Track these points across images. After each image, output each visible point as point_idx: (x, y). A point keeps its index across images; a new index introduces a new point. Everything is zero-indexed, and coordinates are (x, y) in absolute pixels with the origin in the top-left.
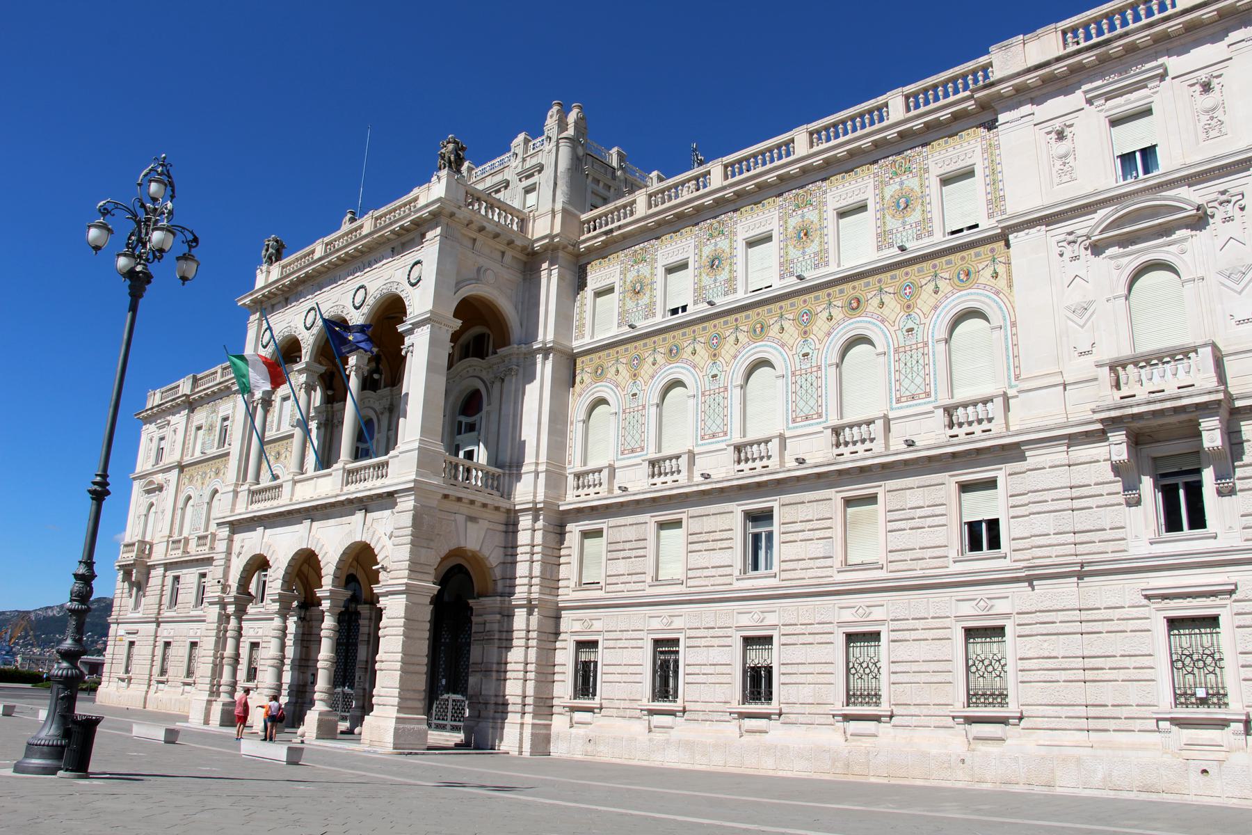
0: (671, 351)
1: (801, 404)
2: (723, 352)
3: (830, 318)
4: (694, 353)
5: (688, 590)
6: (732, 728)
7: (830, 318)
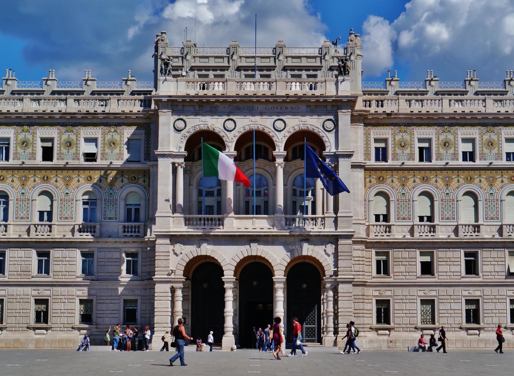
0: (424, 178)
1: (490, 213)
3: (502, 182)
4: (436, 181)
5: (440, 281)
6: (463, 333)
7: (502, 182)
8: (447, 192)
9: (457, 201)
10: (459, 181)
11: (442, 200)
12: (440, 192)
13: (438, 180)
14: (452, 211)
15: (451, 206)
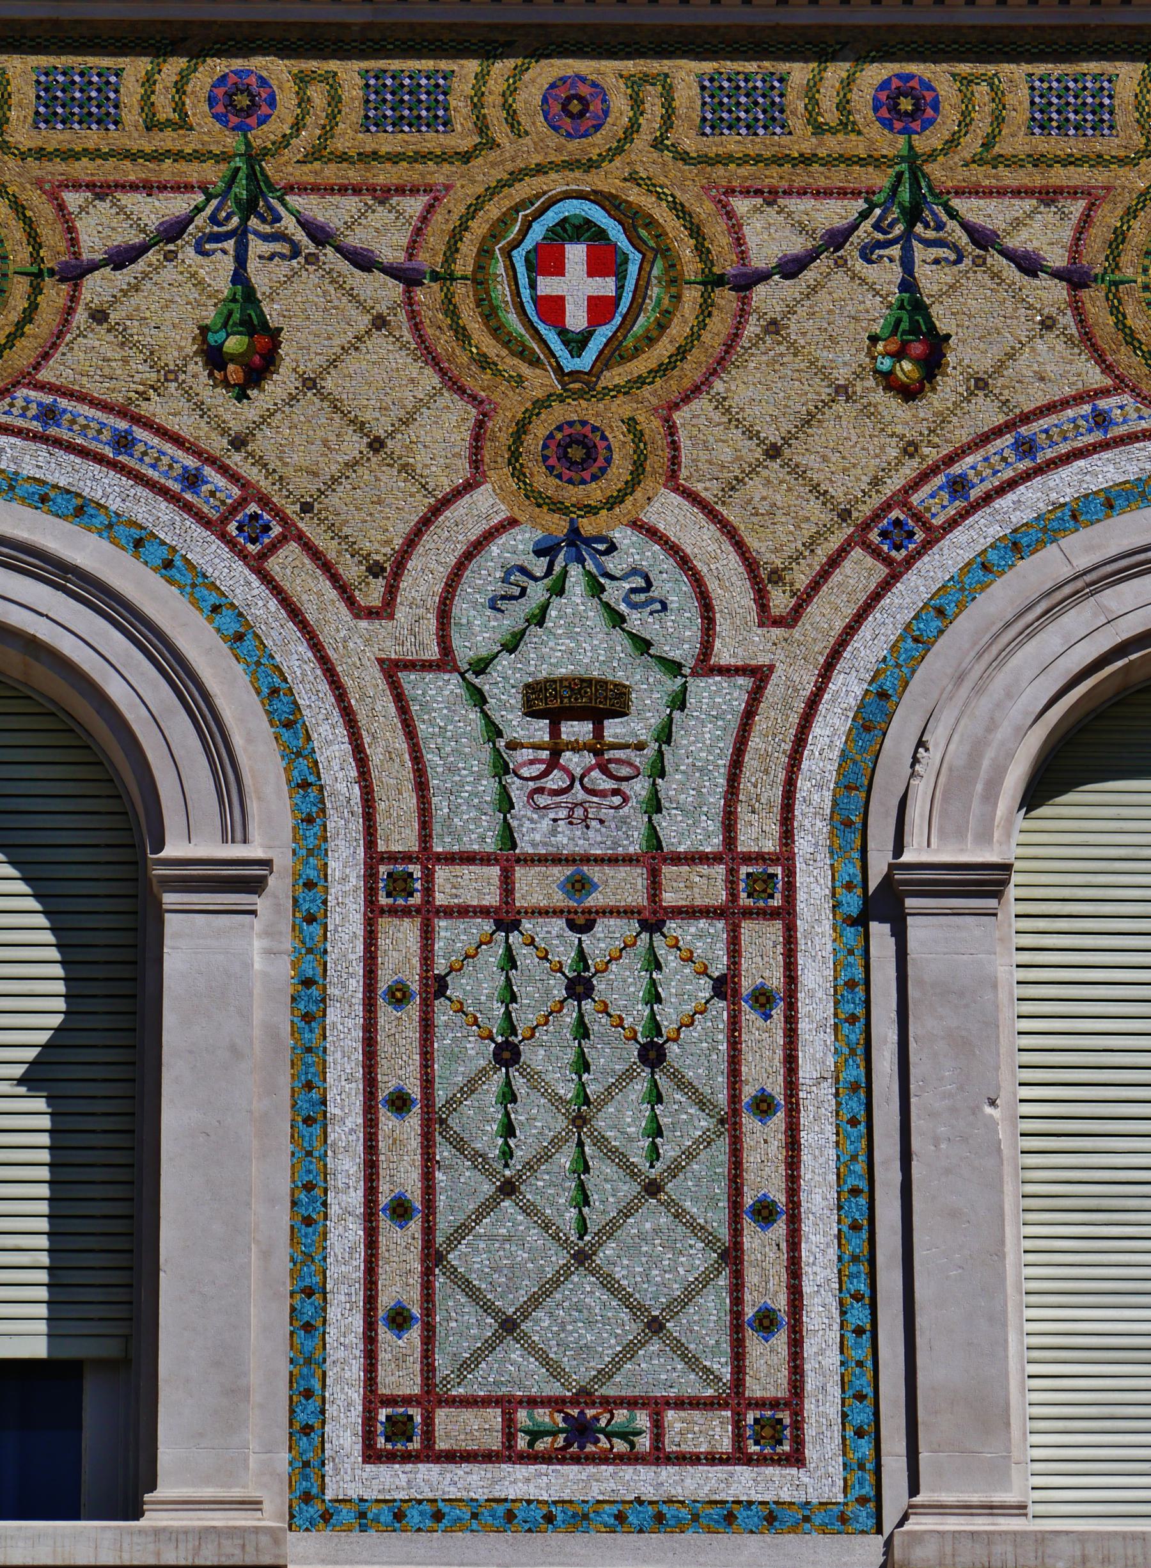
2: (708, 440)
4: (244, 351)
8: (577, 642)
9: (883, 903)
10: (917, 346)
11: (398, 886)
12: (358, 646)
13: (307, 308)
14: (701, 1191)
15: (698, 1055)
